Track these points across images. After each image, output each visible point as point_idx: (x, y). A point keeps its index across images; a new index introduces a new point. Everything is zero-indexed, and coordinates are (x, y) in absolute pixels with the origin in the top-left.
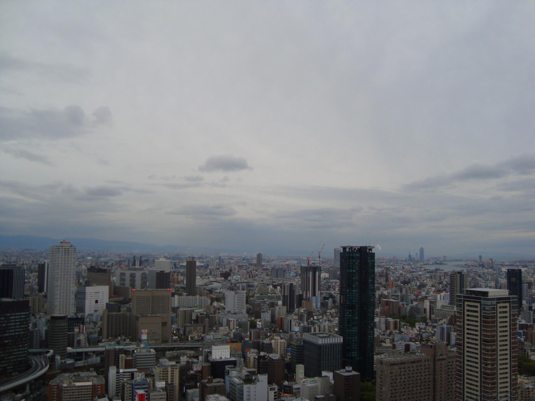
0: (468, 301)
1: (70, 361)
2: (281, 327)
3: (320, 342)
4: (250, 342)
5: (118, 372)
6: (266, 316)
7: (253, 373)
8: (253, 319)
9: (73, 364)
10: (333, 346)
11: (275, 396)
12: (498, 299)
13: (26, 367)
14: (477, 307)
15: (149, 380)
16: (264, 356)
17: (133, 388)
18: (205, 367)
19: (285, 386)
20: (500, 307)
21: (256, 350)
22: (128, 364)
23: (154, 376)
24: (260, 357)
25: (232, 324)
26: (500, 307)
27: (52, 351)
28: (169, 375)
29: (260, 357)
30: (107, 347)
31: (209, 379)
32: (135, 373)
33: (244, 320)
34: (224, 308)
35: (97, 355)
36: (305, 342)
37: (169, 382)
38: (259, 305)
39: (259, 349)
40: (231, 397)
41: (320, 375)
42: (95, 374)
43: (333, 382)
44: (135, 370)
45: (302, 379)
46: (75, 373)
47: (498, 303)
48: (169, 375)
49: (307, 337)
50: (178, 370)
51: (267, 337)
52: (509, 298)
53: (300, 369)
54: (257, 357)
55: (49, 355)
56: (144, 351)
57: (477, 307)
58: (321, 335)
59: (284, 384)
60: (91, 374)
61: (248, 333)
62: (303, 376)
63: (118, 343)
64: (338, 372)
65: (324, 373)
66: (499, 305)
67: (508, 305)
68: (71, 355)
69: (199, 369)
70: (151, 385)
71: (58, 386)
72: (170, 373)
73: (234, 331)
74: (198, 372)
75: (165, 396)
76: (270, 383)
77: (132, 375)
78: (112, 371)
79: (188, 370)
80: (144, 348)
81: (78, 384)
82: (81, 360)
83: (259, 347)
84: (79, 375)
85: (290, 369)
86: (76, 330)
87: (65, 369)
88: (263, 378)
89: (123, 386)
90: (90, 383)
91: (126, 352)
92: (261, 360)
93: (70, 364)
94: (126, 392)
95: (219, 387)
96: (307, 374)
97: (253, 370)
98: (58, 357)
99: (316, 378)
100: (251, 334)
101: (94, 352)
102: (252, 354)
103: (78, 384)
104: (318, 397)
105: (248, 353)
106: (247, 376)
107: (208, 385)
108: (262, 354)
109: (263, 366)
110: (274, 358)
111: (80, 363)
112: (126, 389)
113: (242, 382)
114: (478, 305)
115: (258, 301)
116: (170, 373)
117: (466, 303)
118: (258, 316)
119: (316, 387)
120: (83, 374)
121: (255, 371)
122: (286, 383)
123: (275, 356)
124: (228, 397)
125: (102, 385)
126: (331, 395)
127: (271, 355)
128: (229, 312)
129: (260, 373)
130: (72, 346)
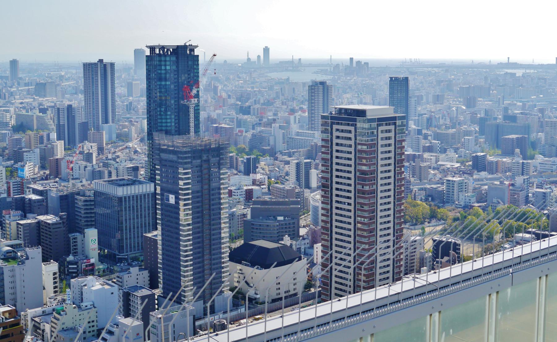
0: (338, 124)
3: (121, 192)
4: (9, 200)
10: (138, 198)
12: (380, 120)
14: (350, 132)
19: (70, 263)
20: (382, 132)
26: (382, 132)
47: (378, 125)
52: (394, 118)
57: (350, 132)
58: (122, 183)
59: (68, 259)
64: (149, 235)
66: (380, 128)
67: (392, 127)
88: (36, 253)
97: (17, 242)
105: (7, 216)
106: (8, 252)
110: (48, 222)
114: (352, 129)
117: (335, 127)
121: (20, 244)
122: (71, 258)
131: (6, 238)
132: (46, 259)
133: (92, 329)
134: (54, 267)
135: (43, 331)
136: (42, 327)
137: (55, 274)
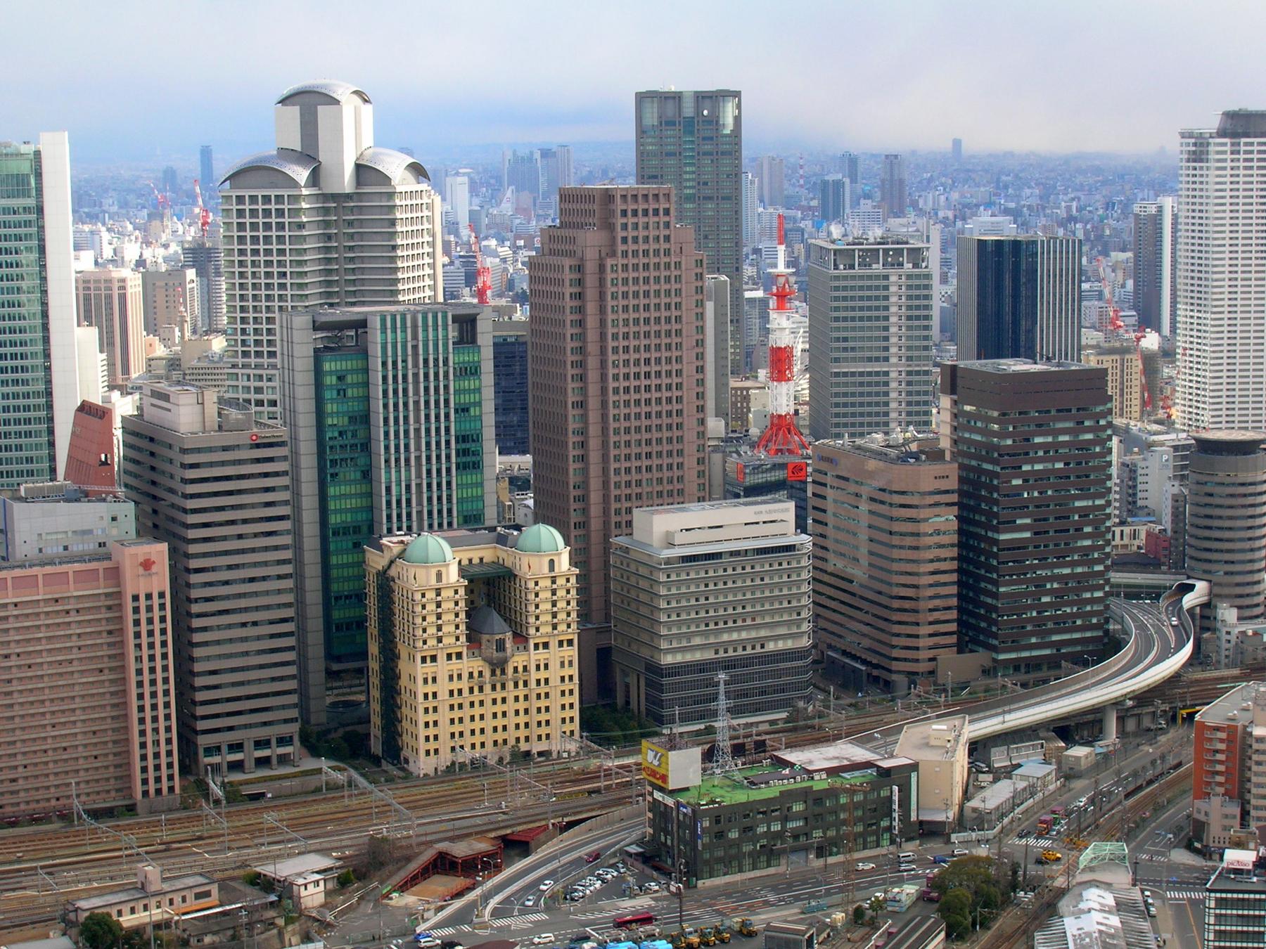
27: (1201, 586)
55: (1189, 600)
71: (1231, 730)
98: (1228, 614)
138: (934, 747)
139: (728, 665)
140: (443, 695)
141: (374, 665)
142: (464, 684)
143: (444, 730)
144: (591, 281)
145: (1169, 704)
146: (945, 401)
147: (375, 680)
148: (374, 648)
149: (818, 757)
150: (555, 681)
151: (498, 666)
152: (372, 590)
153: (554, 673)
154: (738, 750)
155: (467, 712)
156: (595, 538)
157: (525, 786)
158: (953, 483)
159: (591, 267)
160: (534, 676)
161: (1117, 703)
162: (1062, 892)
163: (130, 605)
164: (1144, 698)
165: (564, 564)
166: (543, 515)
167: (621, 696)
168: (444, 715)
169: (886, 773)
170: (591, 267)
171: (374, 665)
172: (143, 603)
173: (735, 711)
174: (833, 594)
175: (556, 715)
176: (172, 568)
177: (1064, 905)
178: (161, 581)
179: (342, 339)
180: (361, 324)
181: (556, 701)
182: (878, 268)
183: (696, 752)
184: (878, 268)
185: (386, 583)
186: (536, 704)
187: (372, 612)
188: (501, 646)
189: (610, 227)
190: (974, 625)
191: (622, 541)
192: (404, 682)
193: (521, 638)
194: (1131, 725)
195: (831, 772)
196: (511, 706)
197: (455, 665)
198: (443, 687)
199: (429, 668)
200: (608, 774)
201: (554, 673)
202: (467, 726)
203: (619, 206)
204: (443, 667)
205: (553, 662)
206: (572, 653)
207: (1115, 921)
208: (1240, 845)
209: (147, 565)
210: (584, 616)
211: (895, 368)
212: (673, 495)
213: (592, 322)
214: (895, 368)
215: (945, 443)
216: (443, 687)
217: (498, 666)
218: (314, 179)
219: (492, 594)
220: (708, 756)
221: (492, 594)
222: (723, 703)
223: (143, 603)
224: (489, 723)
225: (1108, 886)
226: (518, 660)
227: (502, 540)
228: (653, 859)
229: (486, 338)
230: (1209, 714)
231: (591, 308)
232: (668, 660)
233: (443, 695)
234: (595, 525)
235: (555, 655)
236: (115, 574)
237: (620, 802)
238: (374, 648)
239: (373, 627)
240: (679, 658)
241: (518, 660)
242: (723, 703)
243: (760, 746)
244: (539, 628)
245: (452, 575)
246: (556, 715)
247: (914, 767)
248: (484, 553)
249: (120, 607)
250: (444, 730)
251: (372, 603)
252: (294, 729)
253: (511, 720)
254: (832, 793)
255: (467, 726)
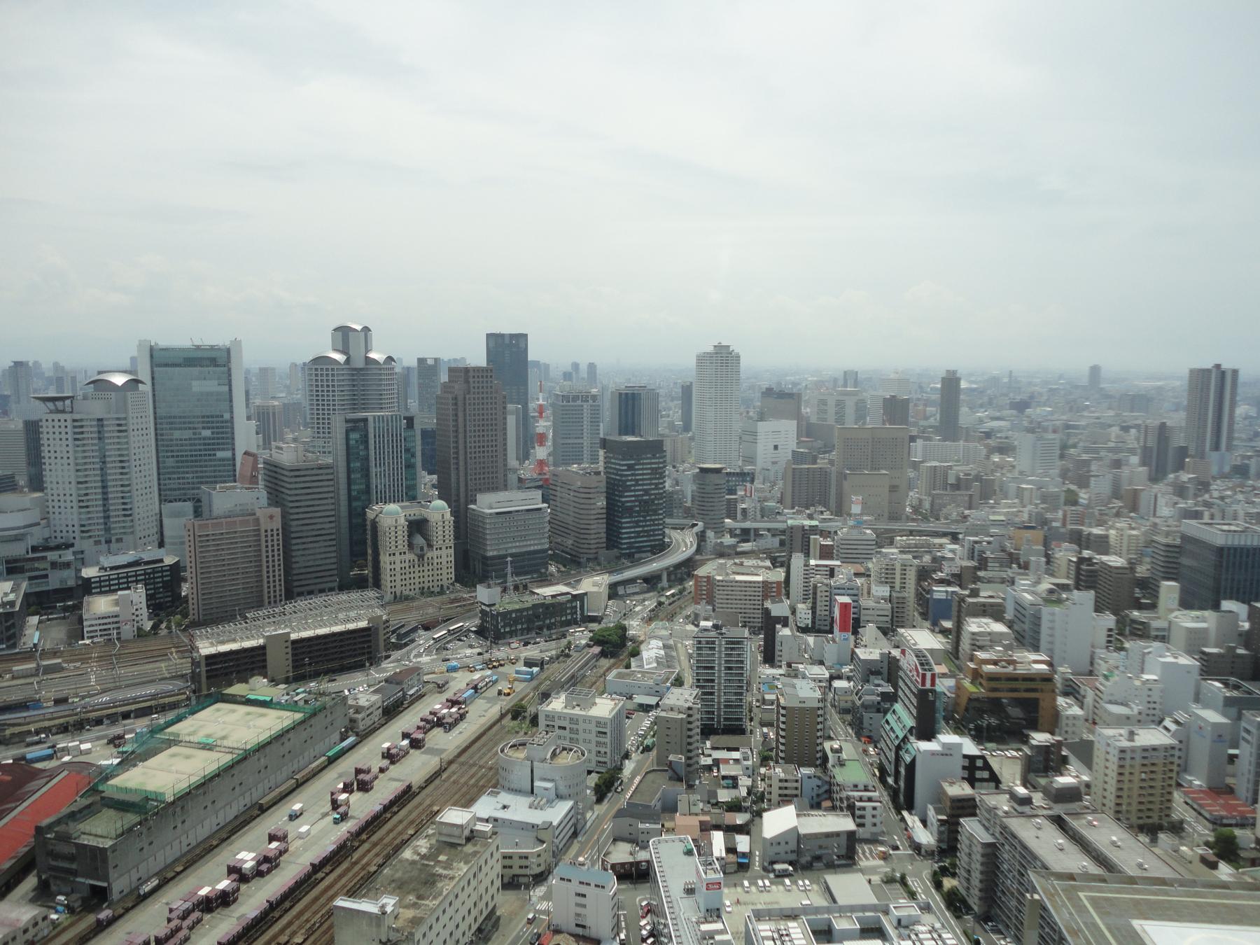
1: (728, 540)
2: (1134, 508)
4: (1063, 530)
5: (806, 565)
6: (1101, 484)
7: (1064, 587)
8: (1073, 487)
9: (734, 546)
11: (1109, 636)
13: (661, 547)
15: (859, 581)
16: (1090, 559)
17: (832, 593)
18: (967, 567)
19: (1134, 621)
21: (1076, 547)
22: (826, 553)
23: (869, 576)
24: (1081, 560)
25: (1026, 494)
28: (898, 576)
29: (1081, 560)
30: (790, 522)
31: (972, 590)
32: (836, 569)
33: (1053, 489)
34: (1014, 467)
35: (773, 536)
36: (1185, 538)
37: (897, 588)
38: (1086, 463)
39: (1080, 545)
40: (1016, 627)
41: (1216, 607)
42: (768, 563)
43: (1246, 626)
44: (838, 563)
45: (1172, 611)
46: (737, 561)
48: (898, 576)
49: (1192, 527)
50: (914, 569)
51: (1100, 524)
53: (1169, 589)
54: (1074, 559)
55: (696, 529)
56: (855, 532)
60: (761, 564)
61: (1060, 514)
62: (1175, 604)
63: (810, 517)
65: (1227, 605)
68: (732, 532)
69: (956, 571)
70: (865, 591)
71: (708, 577)
72: (898, 572)
73: (1030, 507)
74: (953, 575)
75: (889, 613)
76: (1098, 609)
77: (832, 572)
78: (797, 560)
79: (935, 571)
80: (853, 527)
81: (739, 578)
82: (748, 541)
83: (1080, 540)
84: (742, 564)
85: (1148, 586)
86: (741, 493)
87: (721, 553)
89: (815, 587)
90: (760, 579)
91: (825, 534)
92: (1084, 567)
93: (729, 547)
94: (819, 599)
95: (992, 605)
96: (1187, 602)
98: (710, 534)
99: (1207, 613)
100: (1065, 516)
101: (769, 530)
102: (1065, 554)
103: (739, 578)
104: (1207, 650)
106: (1051, 591)
107: (970, 600)
108: (1086, 553)
109: (1086, 576)
111: (746, 546)
112: (819, 594)
113: (1040, 601)
115: (1085, 457)
116: (898, 572)
118: (1083, 482)
119: (1205, 630)
120: (748, 562)
123: (1115, 561)
124: (1010, 627)
125: (778, 583)
126: (1241, 651)
127: (1104, 558)
128: (1021, 473)
129: (1078, 589)
130: (734, 518)
131: (1052, 575)
132: (1098, 609)
133: (1152, 712)
134: (1109, 620)
135: (1084, 697)
136: (1082, 692)
137: (1110, 630)
138: (593, 584)
139: (512, 555)
140: (398, 569)
141: (370, 558)
142: (407, 565)
143: (398, 583)
144: (460, 403)
145: (686, 569)
146: (601, 452)
147: (370, 564)
148: (370, 551)
149: (547, 591)
150: (444, 563)
151: (421, 557)
152: (369, 527)
153: (444, 560)
154: (516, 588)
155: (408, 576)
156: (462, 506)
157: (431, 605)
158: (604, 484)
159: (460, 398)
160: (436, 561)
161: (667, 569)
162: (642, 642)
163: (263, 534)
164: (678, 566)
165: (448, 516)
166: (440, 498)
167: (472, 566)
168: (398, 578)
169: (575, 597)
170: (460, 398)
171: (370, 558)
172: (269, 533)
173: (517, 573)
174: (558, 527)
175: (445, 577)
176: (283, 517)
177: (643, 647)
178: (277, 524)
179: (357, 426)
180: (365, 420)
181: (444, 571)
182: (579, 403)
183: (499, 589)
184: (579, 403)
185: (374, 524)
186: (436, 572)
187: (369, 537)
188: (422, 549)
189: (467, 382)
190: (612, 537)
191: (472, 506)
192: (382, 564)
193: (430, 546)
194: (673, 577)
195: (553, 596)
196: (426, 573)
197: (403, 557)
198: (398, 566)
199: (392, 558)
200: (465, 599)
201: (444, 560)
202: (408, 582)
203: (471, 374)
204: (398, 558)
205: (444, 556)
206: (452, 551)
207: (662, 652)
208: (706, 619)
209: (271, 517)
210: (456, 538)
211: (586, 442)
212: (495, 489)
213: (461, 420)
214: (586, 442)
215: (601, 469)
216: (398, 566)
217: (421, 557)
218: (348, 361)
219: (418, 527)
220: (505, 590)
221: (418, 527)
222: (509, 570)
223: (269, 533)
224: (417, 580)
225: (661, 638)
226: (429, 555)
227: (423, 506)
228: (481, 632)
229: (418, 426)
230: (702, 572)
231: (461, 414)
232: (490, 554)
233: (398, 569)
234: (462, 500)
235: (444, 552)
236: (258, 520)
237: (470, 610)
238: (370, 551)
239: (369, 542)
240: (495, 553)
241: (429, 555)
242: (509, 570)
243: (525, 587)
244: (438, 540)
245: (402, 521)
246: (445, 577)
247: (586, 594)
248: (415, 511)
249: (259, 535)
250: (398, 583)
251: (369, 532)
252: (336, 584)
253: (426, 579)
254: (552, 605)
255: (408, 582)
